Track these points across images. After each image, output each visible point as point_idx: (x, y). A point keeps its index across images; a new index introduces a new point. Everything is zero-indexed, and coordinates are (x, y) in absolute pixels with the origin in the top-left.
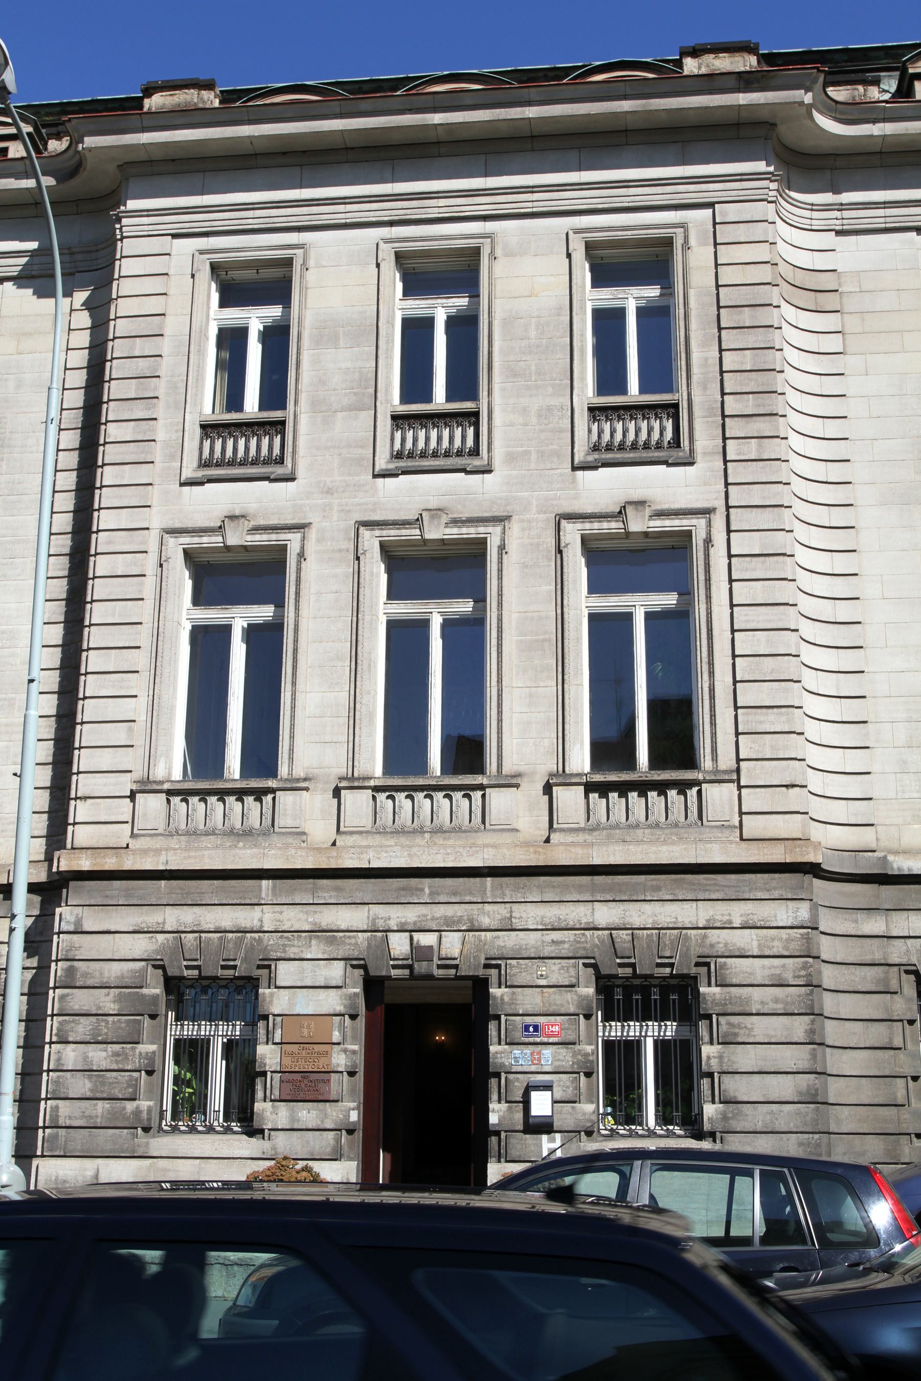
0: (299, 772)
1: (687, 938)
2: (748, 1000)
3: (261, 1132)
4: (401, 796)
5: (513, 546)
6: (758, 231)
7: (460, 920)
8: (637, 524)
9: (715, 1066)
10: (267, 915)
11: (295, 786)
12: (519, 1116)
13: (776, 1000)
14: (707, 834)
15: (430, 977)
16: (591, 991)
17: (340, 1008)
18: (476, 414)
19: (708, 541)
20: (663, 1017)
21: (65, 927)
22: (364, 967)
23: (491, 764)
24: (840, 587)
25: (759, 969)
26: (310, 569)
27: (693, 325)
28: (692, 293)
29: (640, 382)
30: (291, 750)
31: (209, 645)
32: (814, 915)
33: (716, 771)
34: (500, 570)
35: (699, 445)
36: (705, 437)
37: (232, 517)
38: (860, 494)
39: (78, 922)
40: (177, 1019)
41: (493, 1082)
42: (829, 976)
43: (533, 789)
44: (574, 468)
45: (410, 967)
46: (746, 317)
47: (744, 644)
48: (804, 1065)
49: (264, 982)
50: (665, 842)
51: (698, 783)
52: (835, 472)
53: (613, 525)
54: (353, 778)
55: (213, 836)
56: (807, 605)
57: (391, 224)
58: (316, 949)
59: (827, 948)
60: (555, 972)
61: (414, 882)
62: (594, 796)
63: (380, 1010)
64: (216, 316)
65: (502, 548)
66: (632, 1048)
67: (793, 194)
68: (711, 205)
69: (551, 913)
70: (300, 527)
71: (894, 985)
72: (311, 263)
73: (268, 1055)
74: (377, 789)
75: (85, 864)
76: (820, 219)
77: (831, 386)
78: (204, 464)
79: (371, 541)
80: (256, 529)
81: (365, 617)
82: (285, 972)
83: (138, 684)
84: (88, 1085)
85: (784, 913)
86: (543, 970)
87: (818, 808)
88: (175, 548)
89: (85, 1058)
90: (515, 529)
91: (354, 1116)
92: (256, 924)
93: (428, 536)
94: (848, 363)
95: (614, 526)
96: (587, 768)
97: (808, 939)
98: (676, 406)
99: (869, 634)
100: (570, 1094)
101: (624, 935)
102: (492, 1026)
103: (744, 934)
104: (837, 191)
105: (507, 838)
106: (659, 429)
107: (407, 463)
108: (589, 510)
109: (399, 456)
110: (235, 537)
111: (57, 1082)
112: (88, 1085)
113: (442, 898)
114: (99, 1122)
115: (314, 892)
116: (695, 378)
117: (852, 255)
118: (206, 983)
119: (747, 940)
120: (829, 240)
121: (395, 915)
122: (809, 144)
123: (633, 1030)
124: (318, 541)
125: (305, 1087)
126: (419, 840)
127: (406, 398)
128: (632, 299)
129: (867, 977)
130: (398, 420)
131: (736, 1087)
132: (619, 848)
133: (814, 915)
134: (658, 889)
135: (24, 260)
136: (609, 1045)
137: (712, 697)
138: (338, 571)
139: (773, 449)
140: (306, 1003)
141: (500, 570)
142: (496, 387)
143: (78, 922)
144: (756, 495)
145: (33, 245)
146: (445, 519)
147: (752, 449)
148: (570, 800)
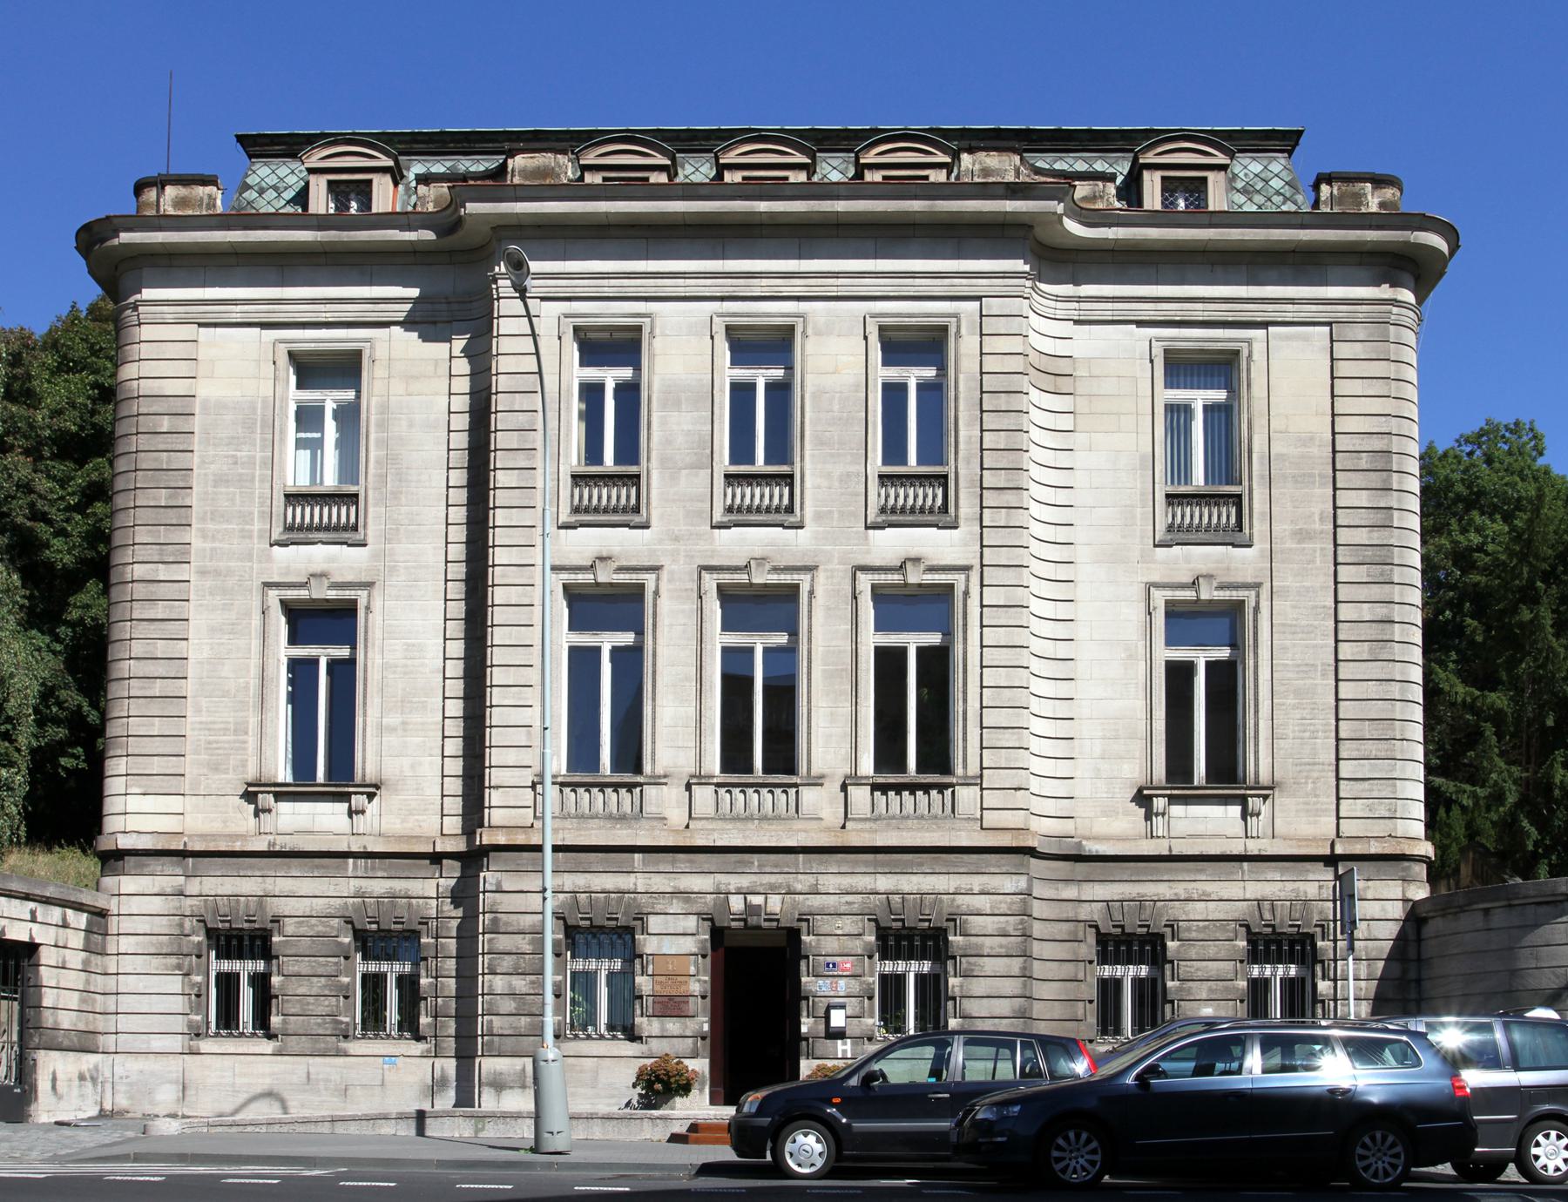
0: (659, 771)
1: (941, 901)
2: (982, 946)
3: (640, 1038)
4: (736, 791)
5: (819, 591)
6: (1014, 325)
7: (780, 886)
8: (915, 577)
9: (957, 992)
10: (640, 880)
11: (657, 781)
12: (822, 1027)
13: (1001, 946)
14: (958, 824)
15: (759, 928)
16: (873, 938)
17: (694, 950)
18: (791, 476)
19: (966, 593)
20: (922, 957)
21: (488, 887)
22: (712, 920)
23: (803, 769)
24: (1060, 631)
25: (990, 924)
26: (665, 604)
27: (961, 407)
28: (961, 377)
29: (920, 452)
30: (653, 753)
31: (583, 663)
32: (1030, 886)
33: (965, 777)
34: (810, 612)
35: (963, 511)
36: (967, 506)
37: (602, 559)
38: (1081, 553)
39: (499, 883)
40: (573, 957)
41: (804, 1003)
42: (1038, 929)
44: (867, 528)
45: (745, 920)
46: (1003, 402)
47: (990, 677)
48: (1018, 992)
49: (639, 930)
50: (928, 830)
51: (952, 785)
52: (1061, 534)
53: (896, 577)
54: (700, 776)
55: (597, 818)
56: (1037, 646)
57: (722, 299)
58: (676, 906)
59: (1038, 909)
60: (848, 925)
61: (746, 856)
62: (877, 794)
63: (721, 951)
64: (579, 374)
65: (811, 593)
66: (900, 980)
67: (1043, 286)
68: (979, 298)
70: (656, 569)
71: (1081, 936)
72: (657, 331)
73: (643, 983)
74: (718, 785)
75: (502, 840)
76: (1063, 309)
77: (1063, 459)
78: (576, 510)
80: (621, 569)
81: (707, 646)
82: (654, 923)
83: (531, 696)
84: (513, 1005)
86: (839, 923)
87: (1038, 805)
88: (556, 582)
89: (510, 985)
90: (821, 576)
91: (706, 1027)
92: (632, 887)
93: (755, 581)
94: (1078, 440)
95: (895, 578)
96: (871, 773)
97: (1024, 902)
98: (946, 477)
99: (1080, 669)
100: (857, 1011)
101: (897, 898)
102: (803, 964)
103: (980, 899)
104: (1077, 283)
105: (814, 825)
106: (933, 496)
107: (738, 516)
108: (878, 563)
109: (730, 510)
110: (605, 576)
111: (490, 1003)
112: (513, 1005)
113: (768, 870)
114: (523, 1031)
115: (673, 862)
116: (961, 454)
117: (1088, 343)
118: (595, 930)
119: (983, 903)
120: (1067, 328)
121: (734, 882)
122: (1058, 241)
123: (901, 966)
124: (669, 581)
125: (671, 1006)
126: (750, 825)
127: (734, 460)
128: (914, 376)
129: (1062, 930)
130: (730, 478)
131: (972, 1007)
132: (895, 833)
133: (1030, 886)
134: (921, 864)
135: (409, 306)
136: (884, 978)
137: (965, 719)
138: (686, 607)
139: (1018, 518)
140: (670, 946)
141: (810, 612)
142: (807, 453)
143: (499, 883)
144: (1003, 557)
145: (414, 292)
146: (768, 567)
147: (1002, 518)
148: (860, 795)
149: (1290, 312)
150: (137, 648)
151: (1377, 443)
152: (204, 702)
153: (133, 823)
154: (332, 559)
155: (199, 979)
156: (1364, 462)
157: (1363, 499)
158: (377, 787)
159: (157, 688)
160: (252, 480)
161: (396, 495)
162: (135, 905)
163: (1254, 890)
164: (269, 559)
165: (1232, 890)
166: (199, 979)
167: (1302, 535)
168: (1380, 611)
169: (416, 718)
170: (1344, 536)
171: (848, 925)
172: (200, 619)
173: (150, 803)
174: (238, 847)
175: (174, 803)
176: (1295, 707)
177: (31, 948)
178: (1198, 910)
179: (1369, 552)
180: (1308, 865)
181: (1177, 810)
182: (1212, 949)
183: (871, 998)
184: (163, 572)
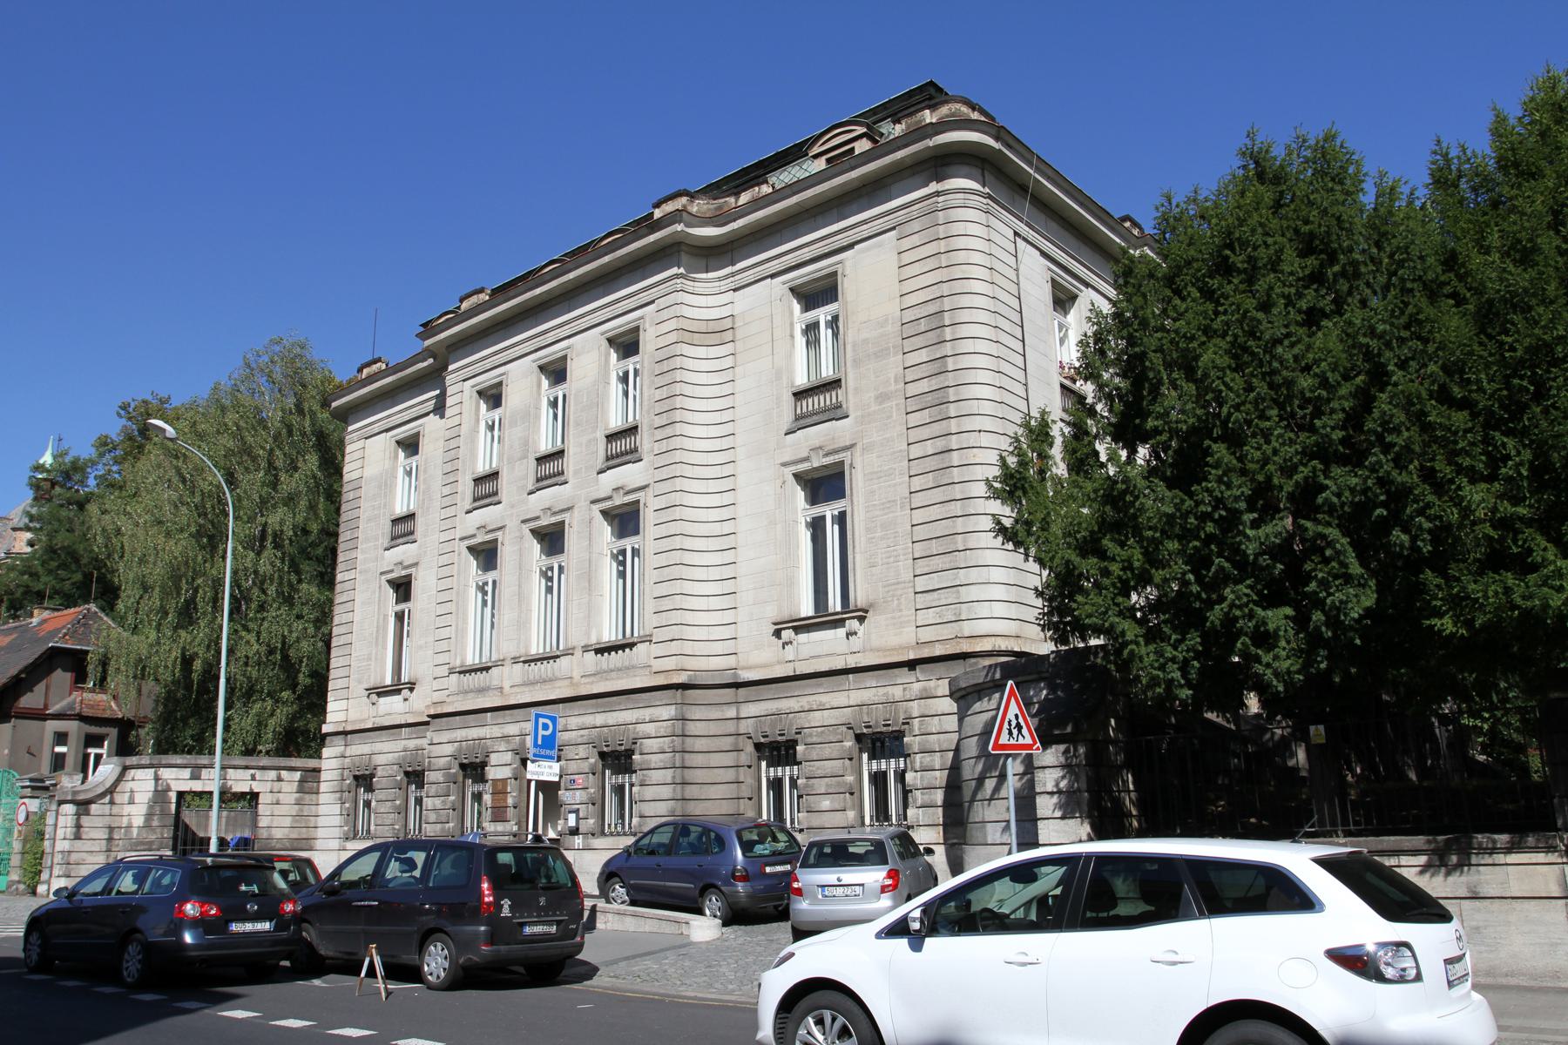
10: (489, 730)
103: (649, 724)
104: (733, 264)
119: (650, 729)
149: (865, 231)
151: (932, 308)
156: (923, 326)
163: (856, 697)
165: (840, 699)
168: (940, 444)
176: (882, 538)
178: (817, 718)
179: (929, 398)
180: (896, 671)
182: (828, 750)
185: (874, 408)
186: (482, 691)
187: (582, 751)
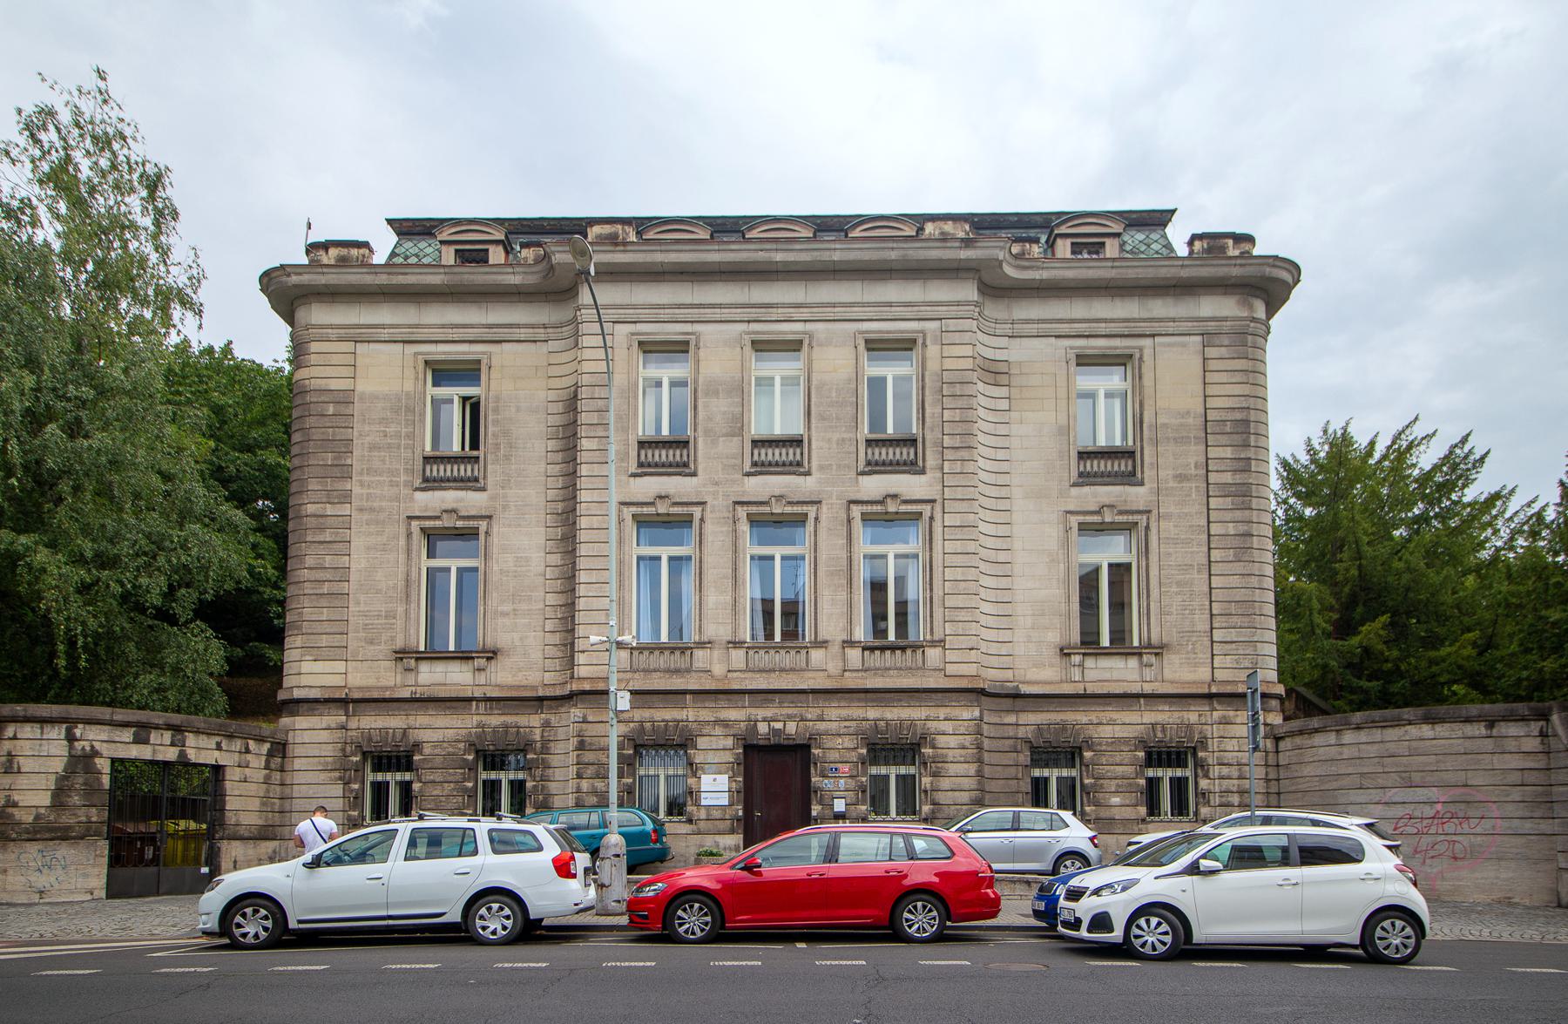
10: (689, 714)
25: (953, 741)
39: (585, 717)
43: (835, 649)
58: (718, 731)
69: (844, 712)
79: (742, 512)
82: (702, 742)
85: (966, 714)
97: (979, 726)
121: (761, 713)
148: (854, 655)
150: (309, 561)
152: (362, 598)
153: (305, 680)
154: (462, 500)
155: (356, 786)
157: (1228, 453)
158: (495, 653)
159: (325, 589)
160: (399, 447)
161: (507, 458)
162: (307, 737)
164: (412, 499)
166: (356, 786)
167: (1181, 478)
169: (524, 606)
170: (1213, 478)
171: (848, 742)
172: (359, 542)
173: (319, 666)
174: (387, 695)
175: (340, 666)
177: (218, 769)
181: (1090, 662)
183: (864, 792)
184: (330, 510)
185: (1171, 484)
186: (677, 671)
187: (848, 742)
